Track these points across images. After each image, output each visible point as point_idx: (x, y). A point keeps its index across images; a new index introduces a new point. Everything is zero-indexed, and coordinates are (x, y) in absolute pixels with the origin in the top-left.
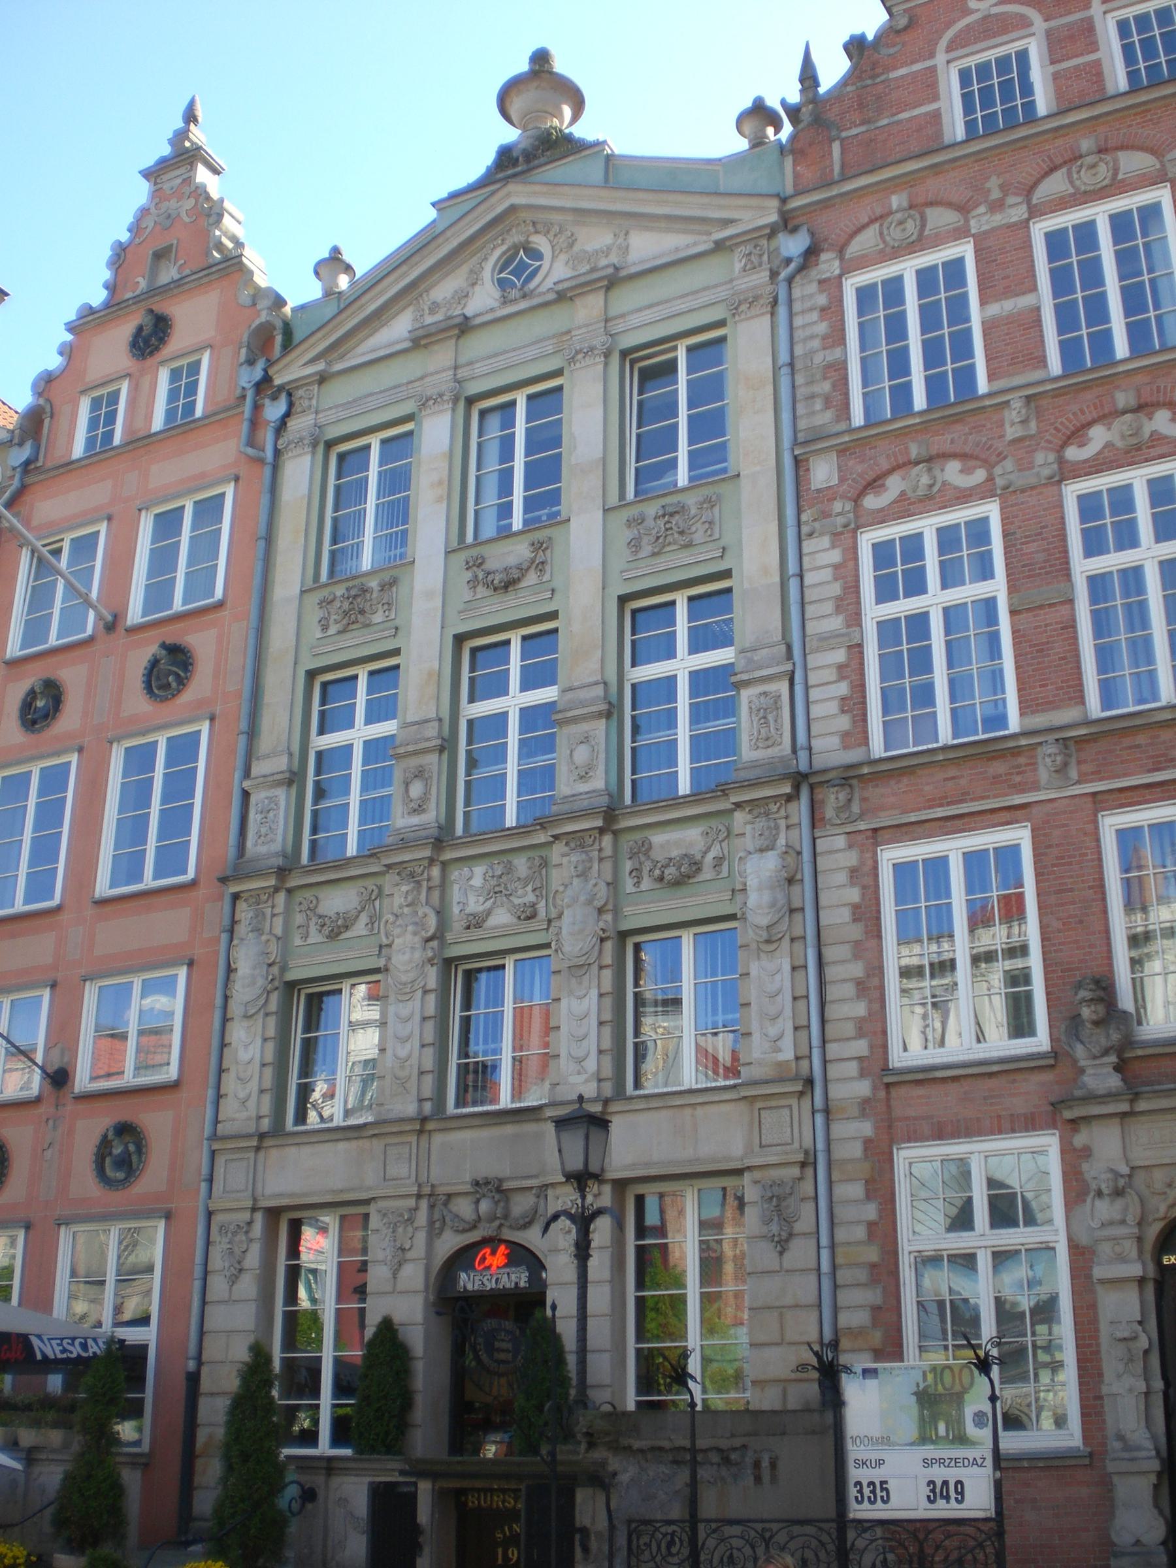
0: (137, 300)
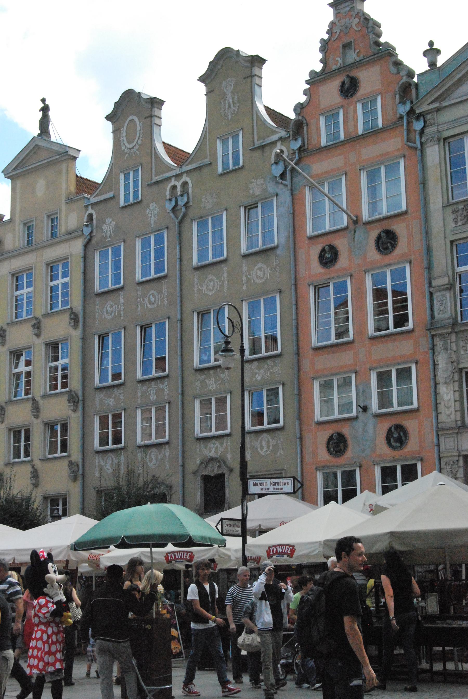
0: (340, 70)
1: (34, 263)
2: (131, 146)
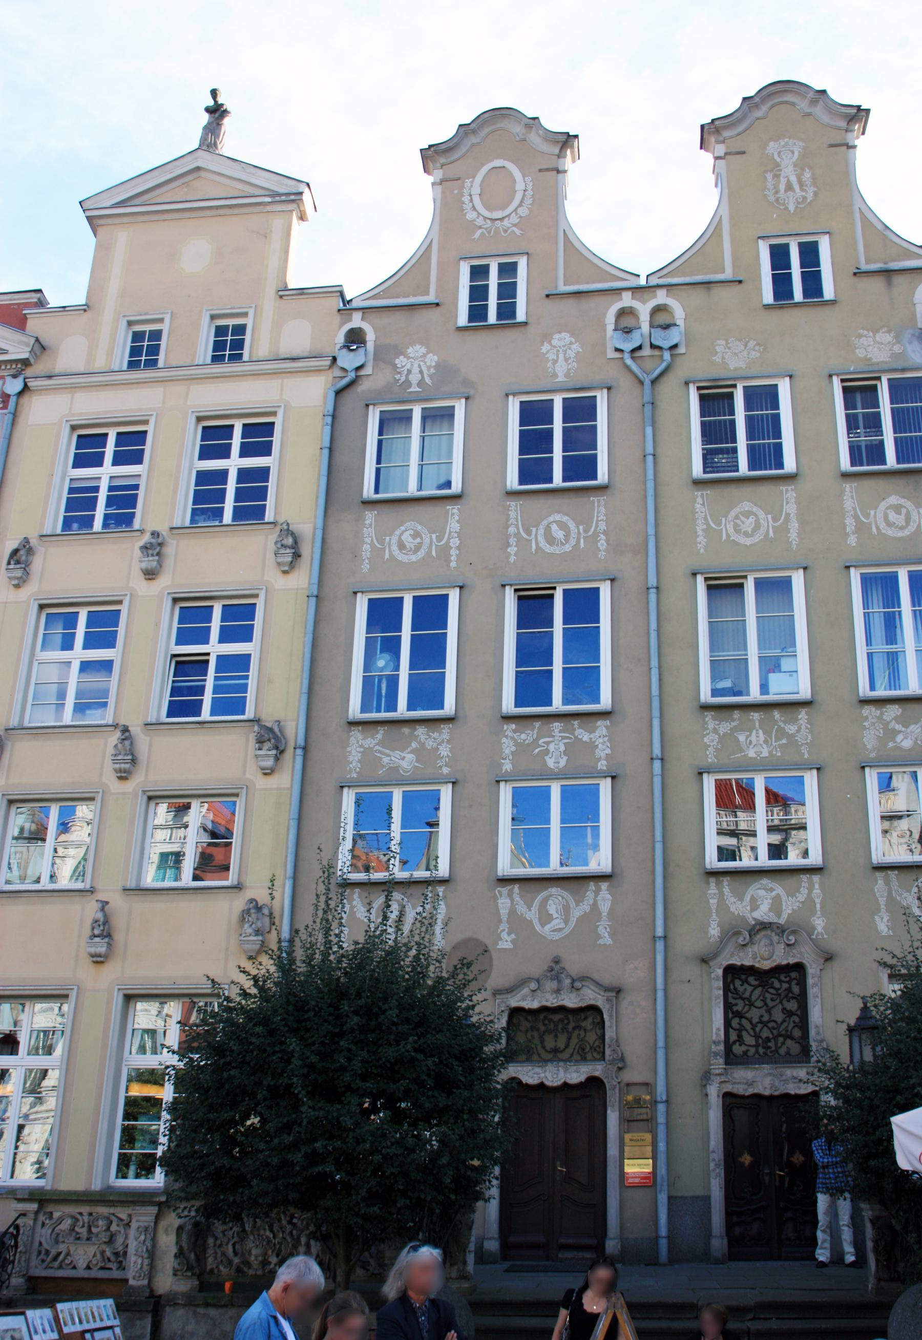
2: (498, 214)
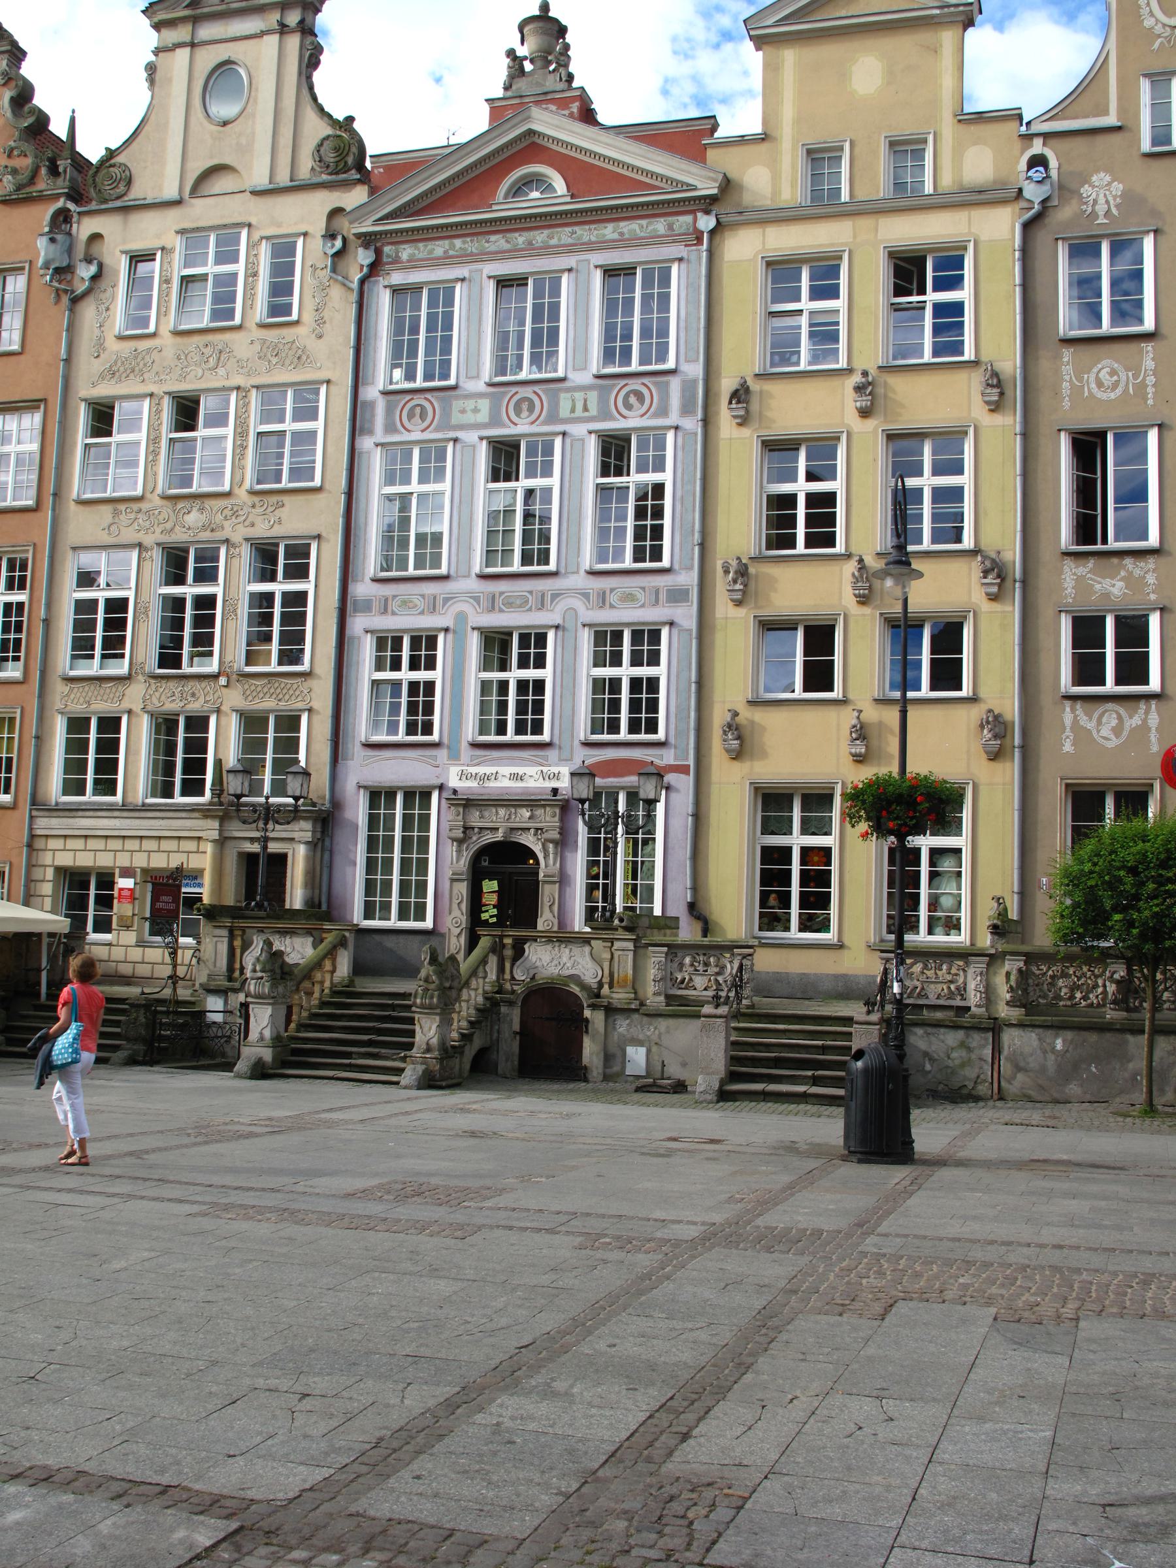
1: (845, 244)
